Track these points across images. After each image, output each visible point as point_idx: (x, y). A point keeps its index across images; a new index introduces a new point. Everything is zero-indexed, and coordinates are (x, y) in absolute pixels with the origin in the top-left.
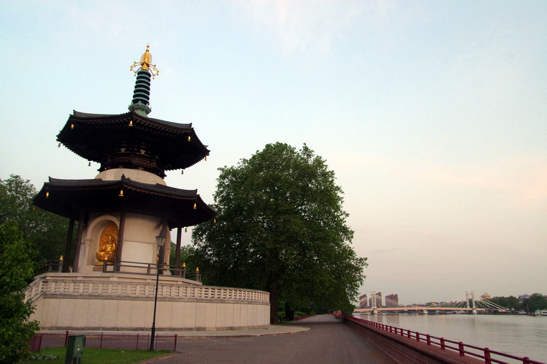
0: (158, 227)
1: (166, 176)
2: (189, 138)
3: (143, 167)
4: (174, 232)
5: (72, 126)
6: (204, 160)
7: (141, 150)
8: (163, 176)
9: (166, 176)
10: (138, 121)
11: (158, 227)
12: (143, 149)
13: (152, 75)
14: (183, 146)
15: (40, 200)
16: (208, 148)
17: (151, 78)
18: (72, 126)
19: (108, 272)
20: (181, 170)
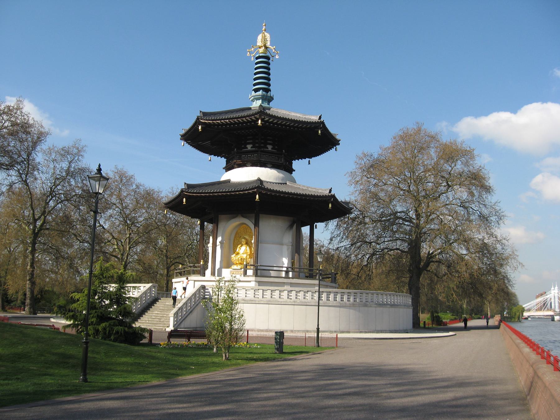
0: (291, 227)
1: (294, 171)
2: (320, 132)
3: (271, 164)
4: (305, 230)
5: (200, 128)
6: (334, 150)
7: (268, 146)
8: (290, 170)
9: (294, 171)
10: (267, 119)
11: (291, 227)
12: (270, 144)
13: (270, 56)
14: (314, 140)
15: (175, 205)
16: (338, 137)
17: (270, 61)
18: (200, 128)
19: (249, 276)
20: (307, 159)
